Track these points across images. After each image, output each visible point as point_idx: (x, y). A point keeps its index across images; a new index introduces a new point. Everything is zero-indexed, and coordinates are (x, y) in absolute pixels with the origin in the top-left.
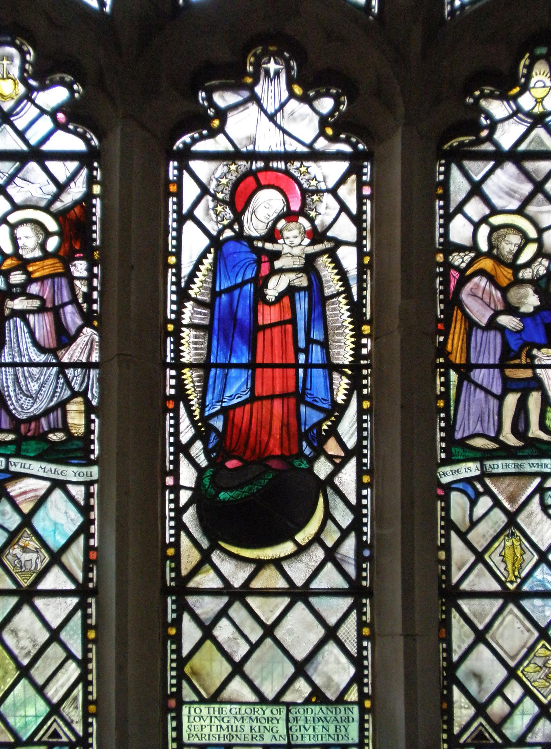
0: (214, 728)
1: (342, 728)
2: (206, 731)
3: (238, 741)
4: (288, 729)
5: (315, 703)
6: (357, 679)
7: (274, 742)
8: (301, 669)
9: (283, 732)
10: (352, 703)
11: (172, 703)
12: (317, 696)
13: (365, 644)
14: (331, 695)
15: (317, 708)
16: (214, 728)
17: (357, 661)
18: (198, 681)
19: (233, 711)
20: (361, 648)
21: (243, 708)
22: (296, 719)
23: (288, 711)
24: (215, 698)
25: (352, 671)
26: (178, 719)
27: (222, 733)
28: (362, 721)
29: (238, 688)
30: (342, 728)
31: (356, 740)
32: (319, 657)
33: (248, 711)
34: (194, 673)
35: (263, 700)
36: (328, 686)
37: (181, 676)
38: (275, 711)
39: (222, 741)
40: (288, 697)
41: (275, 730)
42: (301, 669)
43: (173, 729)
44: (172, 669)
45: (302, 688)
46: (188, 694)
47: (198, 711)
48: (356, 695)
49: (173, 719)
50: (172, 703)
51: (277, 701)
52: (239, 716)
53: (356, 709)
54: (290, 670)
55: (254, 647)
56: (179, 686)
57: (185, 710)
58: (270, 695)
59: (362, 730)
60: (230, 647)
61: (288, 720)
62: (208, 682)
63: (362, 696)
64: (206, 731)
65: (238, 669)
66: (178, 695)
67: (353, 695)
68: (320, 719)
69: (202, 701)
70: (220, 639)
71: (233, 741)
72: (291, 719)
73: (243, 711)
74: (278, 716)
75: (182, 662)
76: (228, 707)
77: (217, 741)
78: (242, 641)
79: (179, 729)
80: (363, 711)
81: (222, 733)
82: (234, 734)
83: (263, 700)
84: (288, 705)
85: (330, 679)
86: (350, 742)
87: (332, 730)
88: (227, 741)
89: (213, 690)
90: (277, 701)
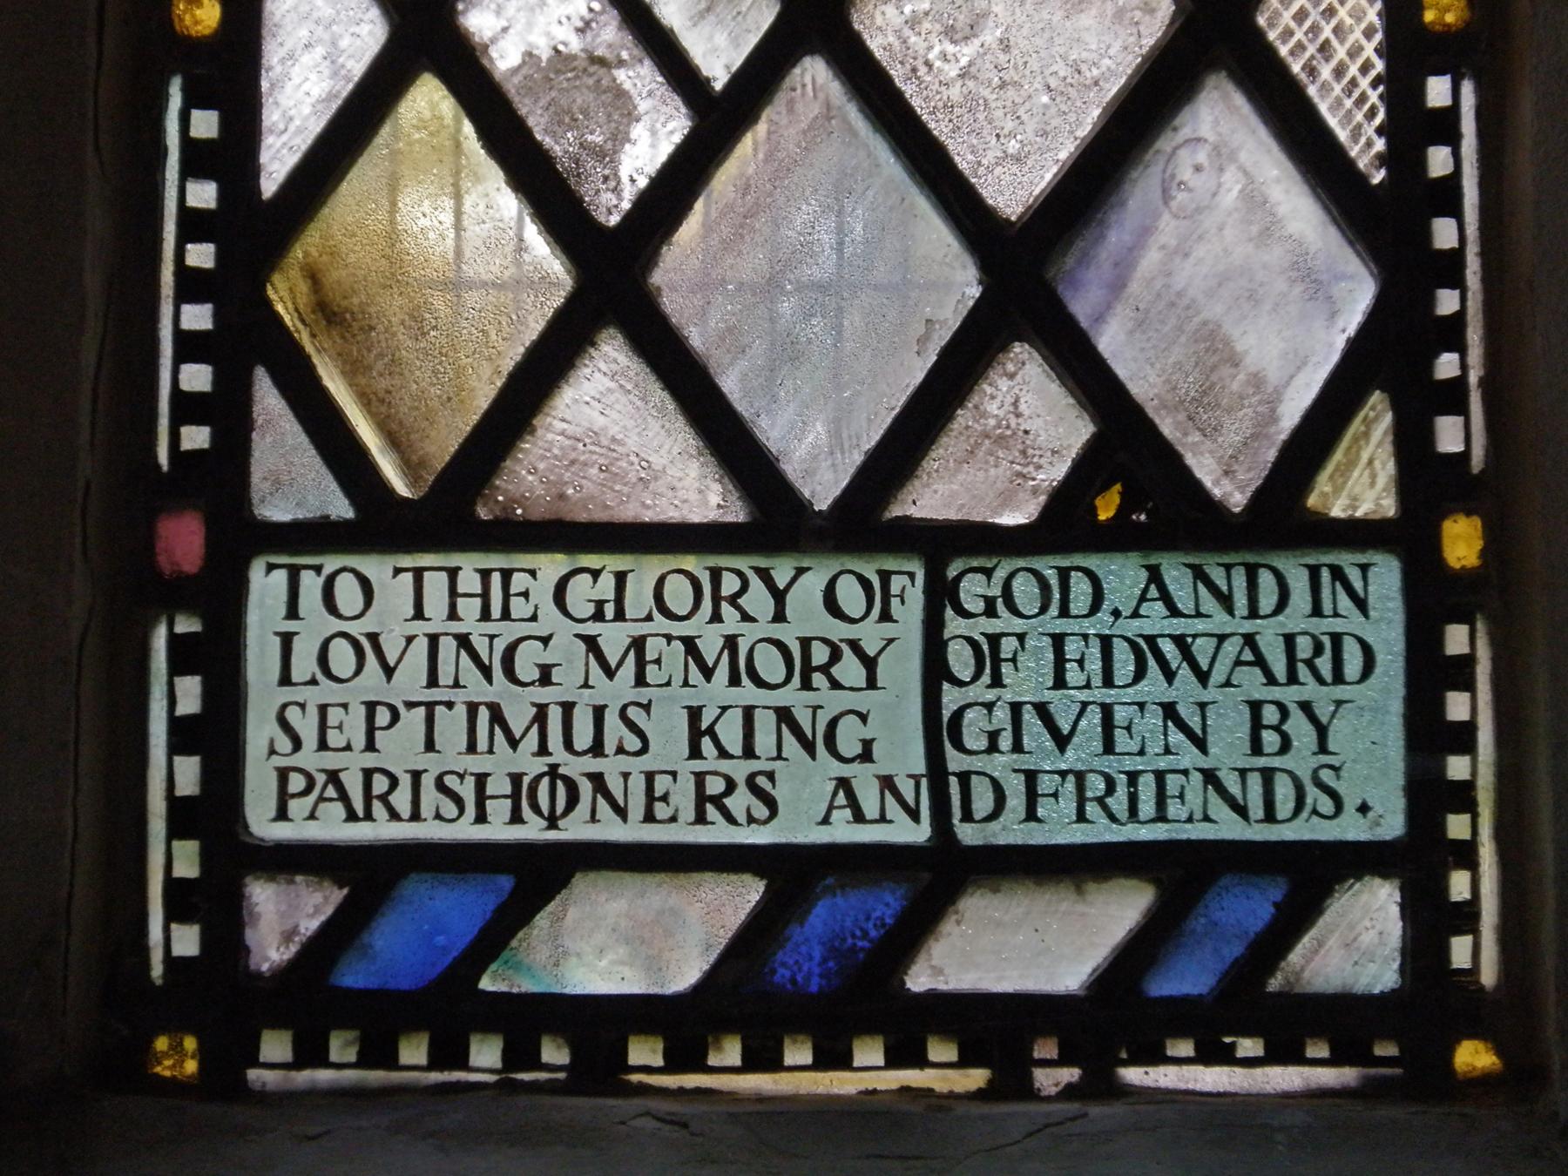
0: (452, 726)
1: (1299, 726)
2: (400, 747)
3: (611, 830)
4: (940, 731)
5: (1115, 538)
6: (1392, 358)
7: (843, 831)
8: (1028, 275)
9: (905, 755)
10: (1361, 534)
11: (183, 541)
12: (1130, 487)
13: (1438, 91)
14: (1226, 474)
15: (1123, 575)
16: (452, 726)
17: (1382, 215)
18: (353, 370)
19: (581, 593)
20: (1412, 127)
21: (645, 571)
22: (989, 657)
23: (941, 595)
24: (457, 509)
25: (1358, 295)
26: (217, 657)
27: (500, 764)
28: (1430, 673)
29: (612, 431)
30: (1299, 726)
31: (1391, 823)
32: (1141, 189)
33: (679, 595)
34: (329, 313)
35: (772, 516)
36: (1202, 405)
37: (249, 341)
38: (850, 596)
39: (498, 830)
40: (933, 496)
41: (849, 737)
42: (1028, 275)
43: (183, 735)
44: (192, 286)
45: (1029, 425)
46: (289, 477)
47: (348, 593)
48: (1387, 469)
49: (183, 657)
50: (183, 541)
51: (863, 519)
52: (614, 638)
53: (1385, 577)
54: (960, 284)
55: (720, 117)
56: (228, 412)
57: (265, 585)
58: (822, 480)
59: (1430, 736)
60: (564, 118)
61: (935, 671)
62: (420, 380)
63: (1427, 482)
64: (400, 747)
65: (612, 279)
66: (222, 476)
67: (1361, 483)
68: (1146, 650)
69: (380, 524)
70: (504, 59)
71: (575, 829)
72: (960, 659)
73: (639, 597)
74: (871, 635)
75: (257, 229)
76: (552, 566)
77: (465, 830)
78: (641, 79)
79: (215, 735)
80: (1432, 598)
81: (500, 764)
82: (574, 767)
83: (772, 516)
84: (945, 544)
85: (1216, 350)
86: (1351, 829)
87: (1228, 746)
88: (533, 830)
89: (445, 440)
90: (863, 519)
